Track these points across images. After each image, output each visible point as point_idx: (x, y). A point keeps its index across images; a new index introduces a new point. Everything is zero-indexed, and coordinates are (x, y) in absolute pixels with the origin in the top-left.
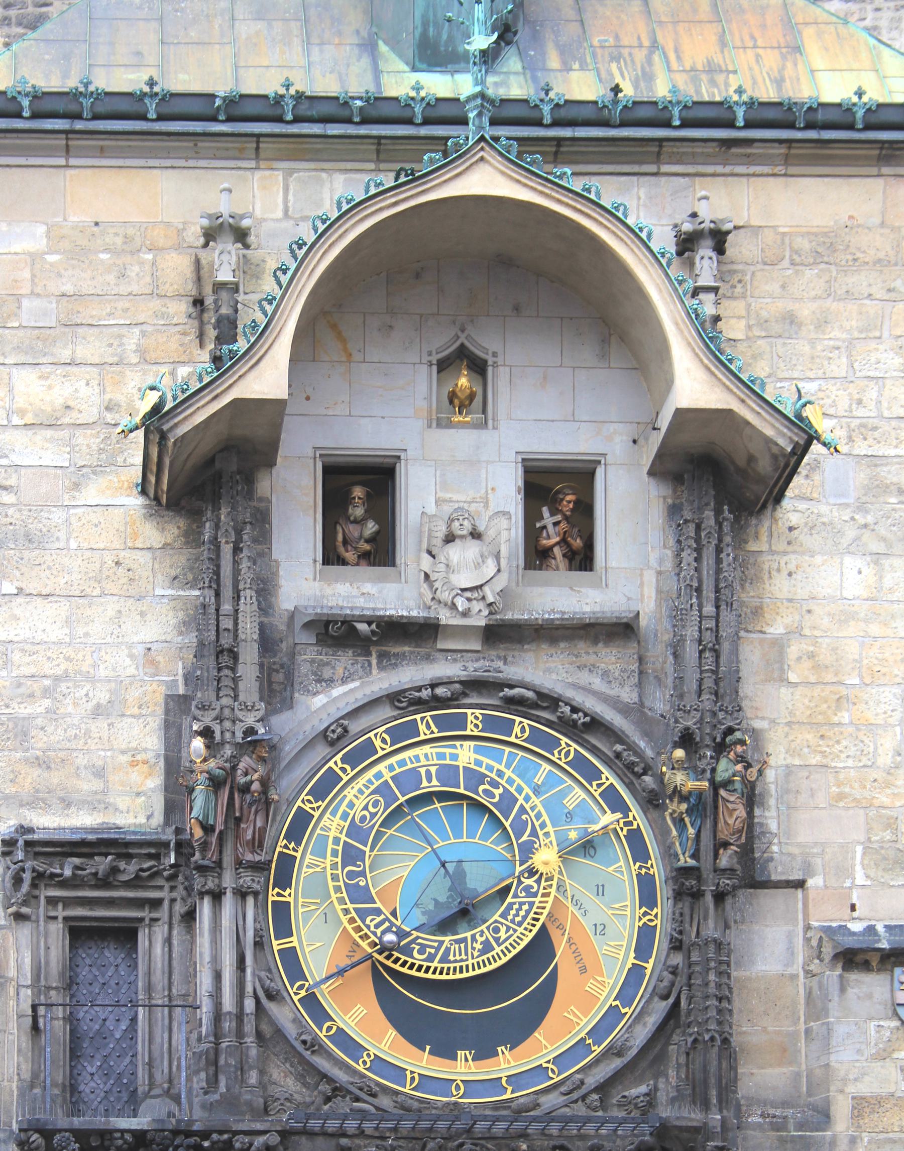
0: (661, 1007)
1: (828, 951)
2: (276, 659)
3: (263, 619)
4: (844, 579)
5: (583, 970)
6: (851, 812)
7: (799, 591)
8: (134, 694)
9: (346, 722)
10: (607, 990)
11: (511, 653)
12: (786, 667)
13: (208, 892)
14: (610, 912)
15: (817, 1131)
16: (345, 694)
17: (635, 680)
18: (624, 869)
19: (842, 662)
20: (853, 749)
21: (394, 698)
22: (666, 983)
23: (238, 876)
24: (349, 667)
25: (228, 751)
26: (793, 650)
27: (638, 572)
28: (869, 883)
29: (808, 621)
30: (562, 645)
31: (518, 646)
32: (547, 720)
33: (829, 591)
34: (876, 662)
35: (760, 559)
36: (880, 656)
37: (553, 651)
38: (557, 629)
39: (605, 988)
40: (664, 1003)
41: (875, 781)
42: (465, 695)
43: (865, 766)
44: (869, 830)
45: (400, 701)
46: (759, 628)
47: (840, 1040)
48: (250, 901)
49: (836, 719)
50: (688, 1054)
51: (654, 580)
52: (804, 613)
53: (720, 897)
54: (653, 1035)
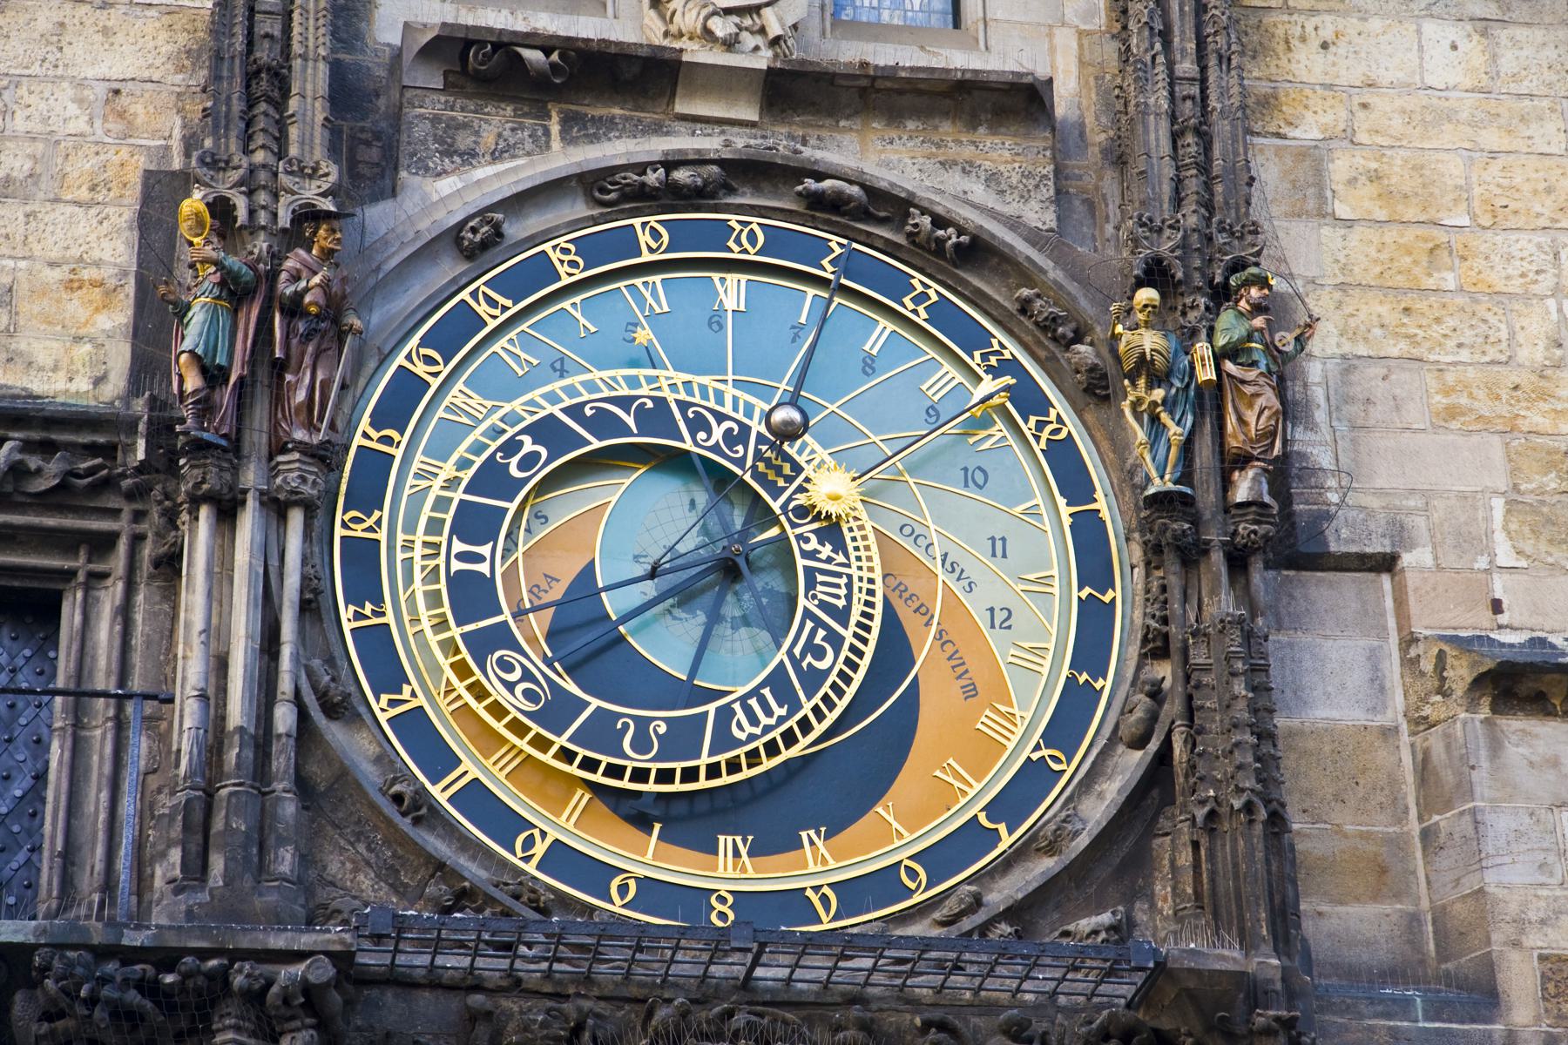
0: (1131, 763)
1: (1461, 673)
2: (367, 124)
3: (341, 56)
4: (1427, 58)
5: (971, 691)
6: (1475, 438)
7: (1343, 72)
8: (83, 165)
9: (499, 216)
10: (1020, 731)
11: (813, 133)
12: (1329, 194)
13: (209, 498)
14: (1020, 587)
15: (1473, 1021)
16: (497, 175)
17: (1049, 191)
18: (1043, 510)
19: (1437, 191)
20: (1469, 333)
21: (591, 183)
22: (1139, 713)
23: (273, 471)
24: (506, 133)
25: (261, 244)
26: (1340, 167)
27: (1044, 30)
28: (1523, 563)
29: (1362, 121)
30: (911, 125)
31: (828, 122)
32: (887, 240)
33: (1400, 75)
34: (1499, 191)
35: (1269, 19)
36: (1505, 182)
37: (894, 134)
38: (901, 92)
39: (1019, 725)
40: (1139, 754)
41: (1516, 388)
42: (732, 191)
43: (1493, 362)
44: (1515, 471)
45: (603, 190)
46: (1273, 129)
47: (1502, 843)
48: (296, 518)
49: (1430, 283)
50: (1196, 845)
51: (1075, 45)
52: (1356, 108)
53: (1238, 561)
54: (1120, 812)
